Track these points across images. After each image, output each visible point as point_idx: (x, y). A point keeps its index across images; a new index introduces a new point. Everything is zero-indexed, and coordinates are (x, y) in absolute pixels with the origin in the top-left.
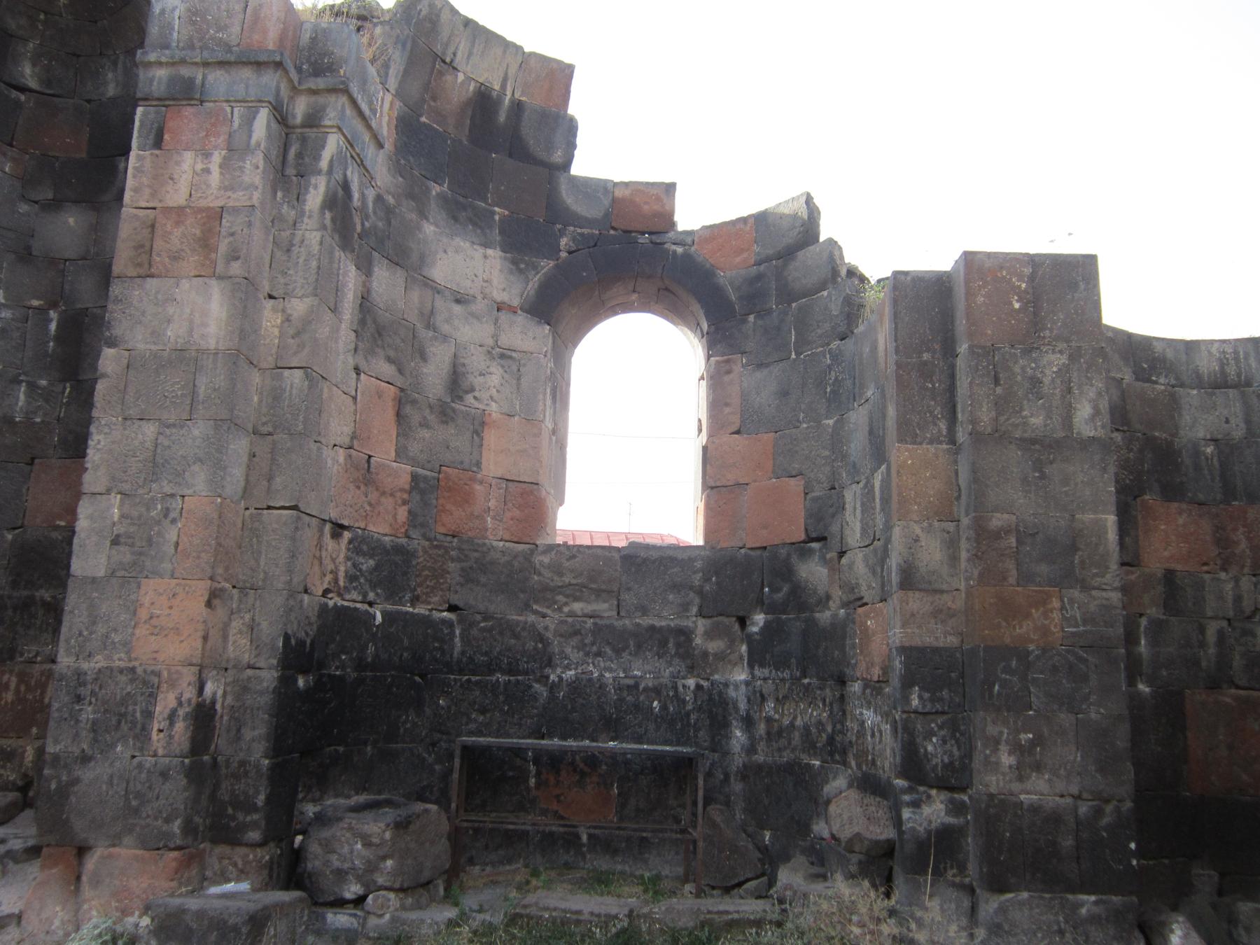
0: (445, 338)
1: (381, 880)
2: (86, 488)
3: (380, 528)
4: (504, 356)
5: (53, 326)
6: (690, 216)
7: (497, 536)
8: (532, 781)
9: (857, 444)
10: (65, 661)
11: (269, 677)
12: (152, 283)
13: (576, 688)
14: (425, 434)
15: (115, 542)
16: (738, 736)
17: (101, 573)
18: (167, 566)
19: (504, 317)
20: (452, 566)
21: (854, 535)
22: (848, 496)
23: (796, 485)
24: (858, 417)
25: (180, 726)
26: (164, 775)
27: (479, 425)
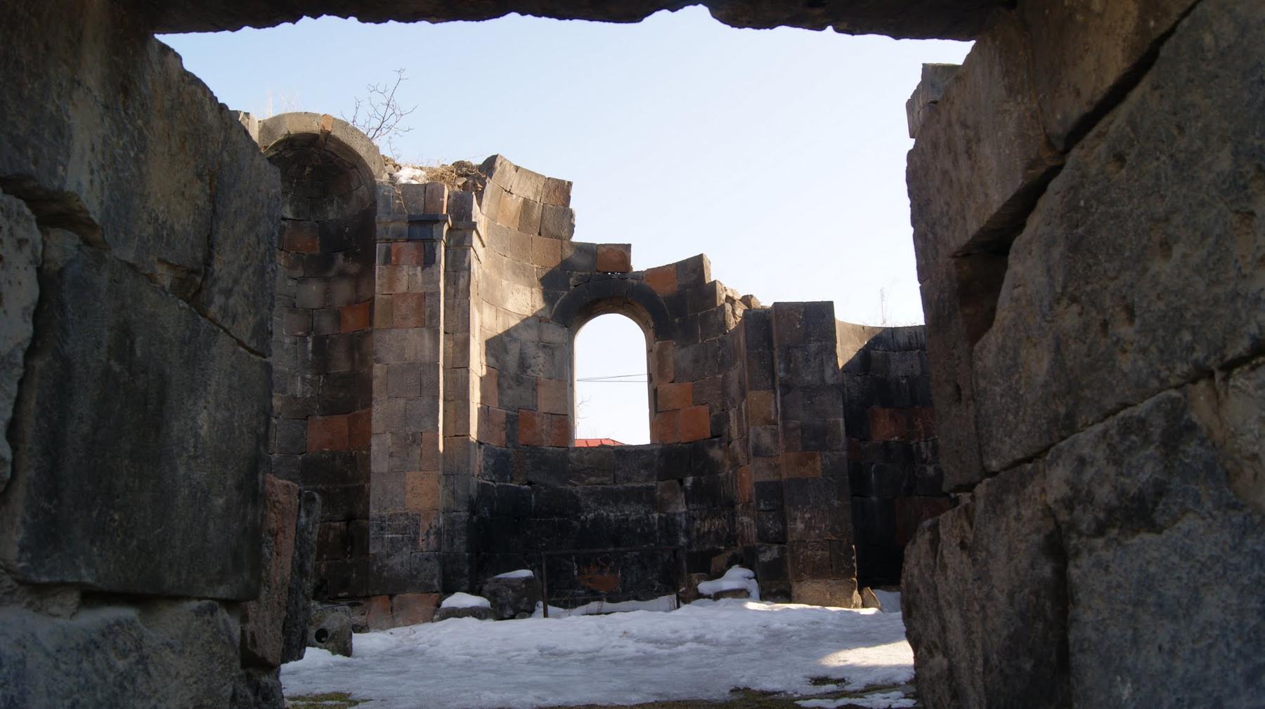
0: (515, 340)
1: (522, 607)
2: (374, 431)
3: (494, 444)
4: (546, 346)
5: (310, 345)
6: (639, 263)
7: (548, 444)
8: (576, 572)
9: (734, 389)
10: (373, 512)
11: (464, 515)
12: (394, 332)
13: (594, 521)
14: (509, 392)
15: (391, 456)
16: (683, 540)
17: (386, 470)
18: (417, 465)
19: (544, 325)
20: (528, 461)
21: (734, 433)
22: (731, 414)
23: (705, 409)
24: (734, 374)
25: (432, 537)
26: (427, 559)
27: (535, 385)
